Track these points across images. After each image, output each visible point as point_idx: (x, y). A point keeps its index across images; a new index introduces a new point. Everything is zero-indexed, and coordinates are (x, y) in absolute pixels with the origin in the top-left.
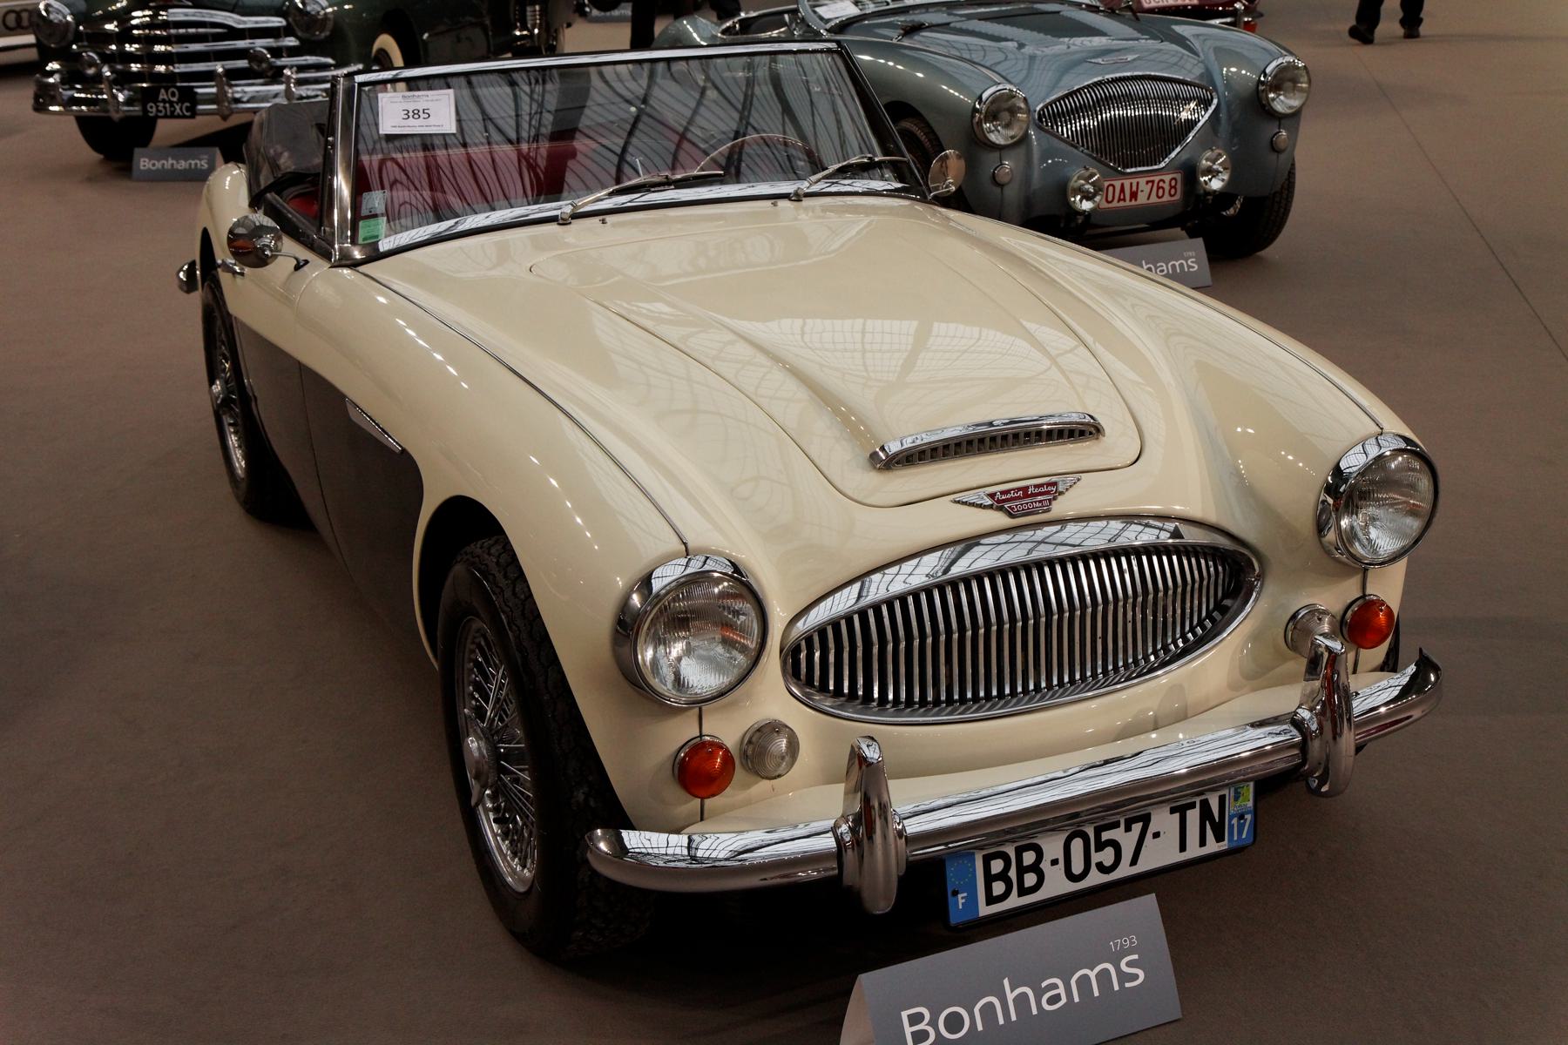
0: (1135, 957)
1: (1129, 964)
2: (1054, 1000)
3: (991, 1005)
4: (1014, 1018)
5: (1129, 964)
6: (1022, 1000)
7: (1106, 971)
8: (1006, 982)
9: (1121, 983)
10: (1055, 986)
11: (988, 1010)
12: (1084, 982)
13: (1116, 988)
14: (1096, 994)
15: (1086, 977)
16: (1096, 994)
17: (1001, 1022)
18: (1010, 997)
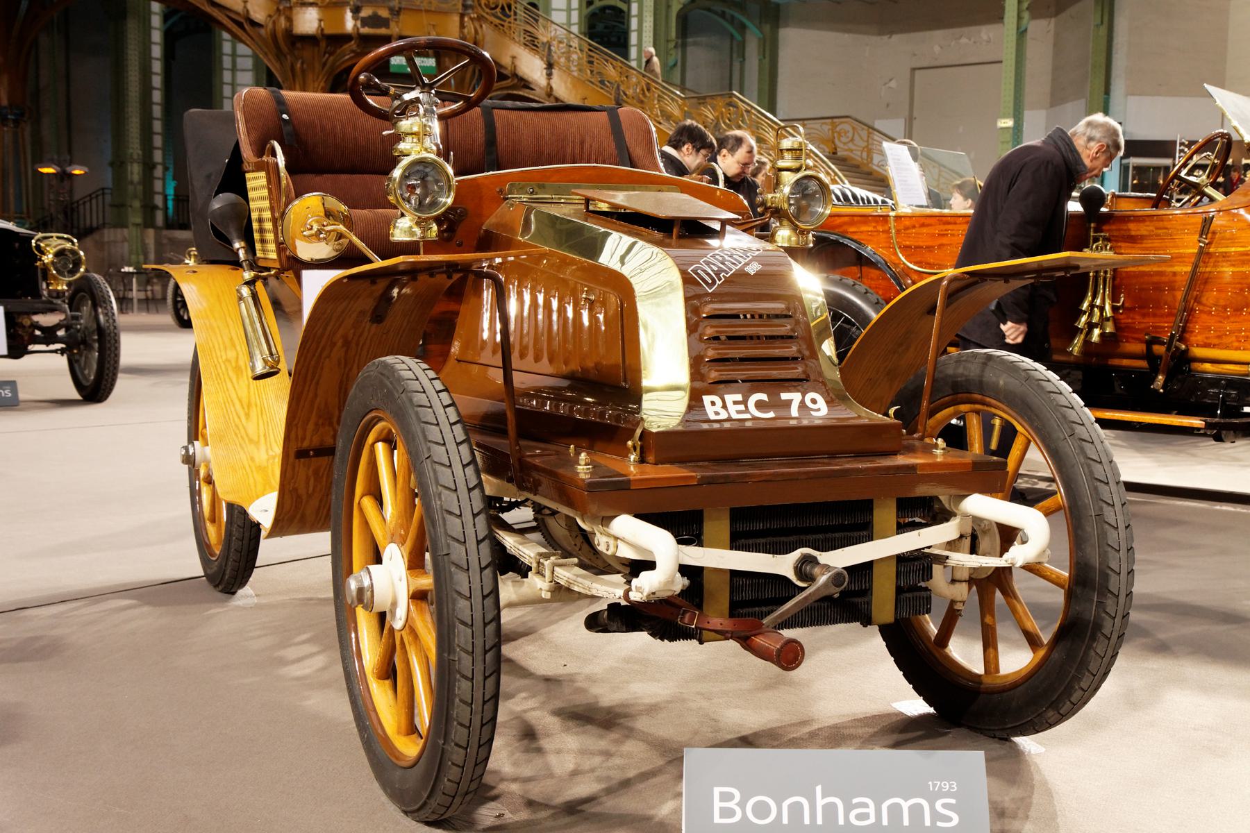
0: (953, 801)
1: (944, 806)
2: (861, 817)
4: (820, 821)
5: (944, 806)
6: (830, 810)
7: (920, 806)
8: (819, 789)
9: (933, 821)
10: (866, 805)
11: (796, 809)
12: (895, 811)
13: (928, 823)
14: (906, 822)
16: (906, 822)
17: (807, 821)
18: (820, 802)
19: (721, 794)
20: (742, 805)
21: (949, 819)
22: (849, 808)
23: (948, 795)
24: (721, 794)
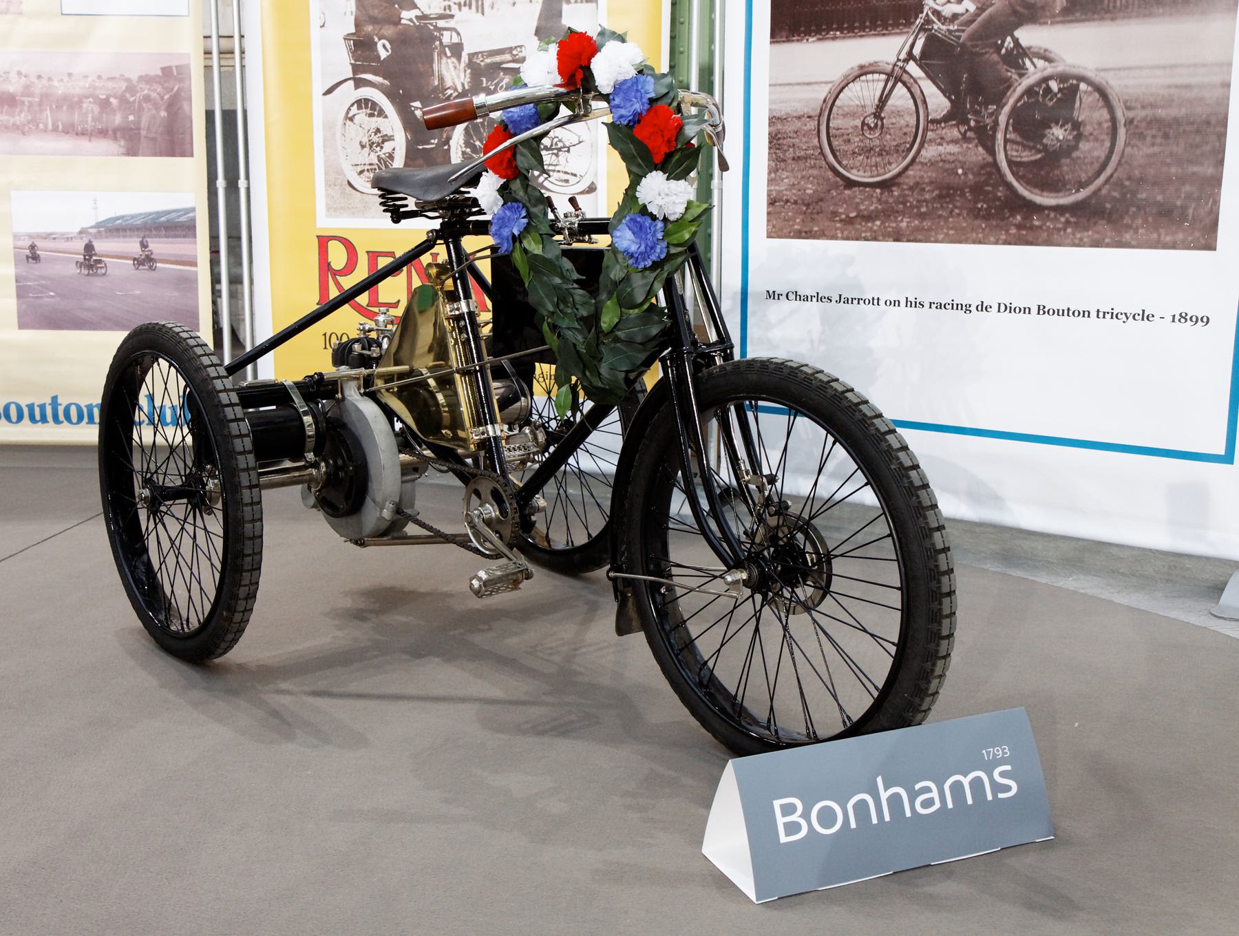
0: (1008, 768)
1: (1002, 774)
2: (928, 803)
3: (863, 802)
4: (887, 818)
5: (1002, 774)
6: (895, 801)
7: (979, 779)
10: (928, 790)
11: (861, 807)
12: (957, 787)
13: (990, 797)
14: (970, 801)
16: (970, 801)
17: (875, 821)
18: (884, 796)
19: (782, 806)
20: (806, 815)
22: (913, 796)
24: (782, 806)
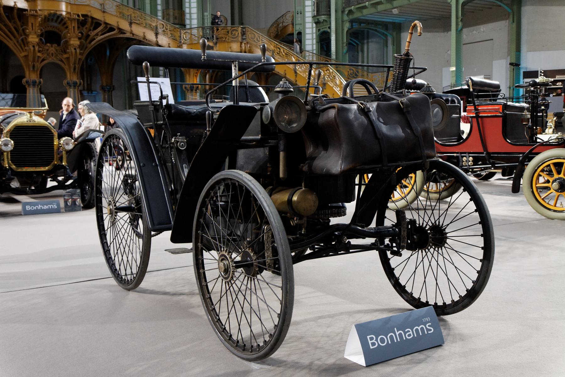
1: (429, 326)
2: (409, 335)
3: (392, 335)
5: (429, 326)
6: (400, 335)
7: (422, 329)
9: (427, 332)
10: (409, 331)
11: (391, 337)
12: (417, 330)
15: (417, 329)
18: (397, 334)
19: (370, 338)
20: (377, 340)
21: (431, 330)
22: (405, 333)
23: (428, 322)
24: (370, 338)
